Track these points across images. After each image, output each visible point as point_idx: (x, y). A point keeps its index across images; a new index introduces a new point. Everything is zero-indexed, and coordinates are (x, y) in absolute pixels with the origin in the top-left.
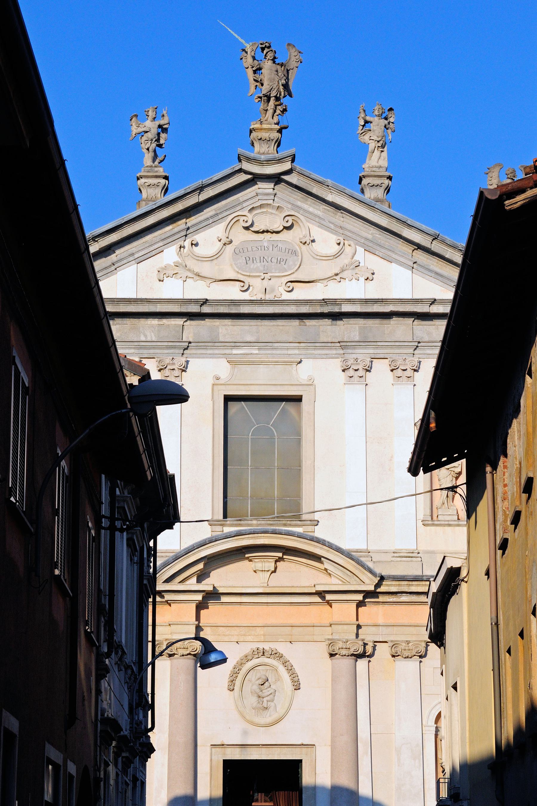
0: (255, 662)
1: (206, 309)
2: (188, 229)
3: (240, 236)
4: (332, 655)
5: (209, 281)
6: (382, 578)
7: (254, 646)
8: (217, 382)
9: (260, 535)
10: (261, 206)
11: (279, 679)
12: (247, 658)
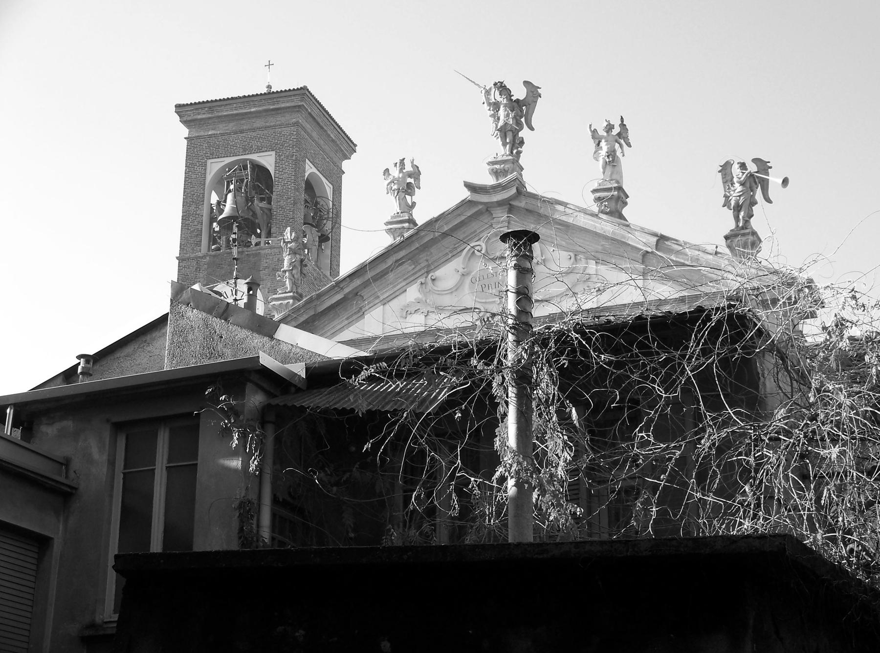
2: (429, 266)
3: (479, 265)
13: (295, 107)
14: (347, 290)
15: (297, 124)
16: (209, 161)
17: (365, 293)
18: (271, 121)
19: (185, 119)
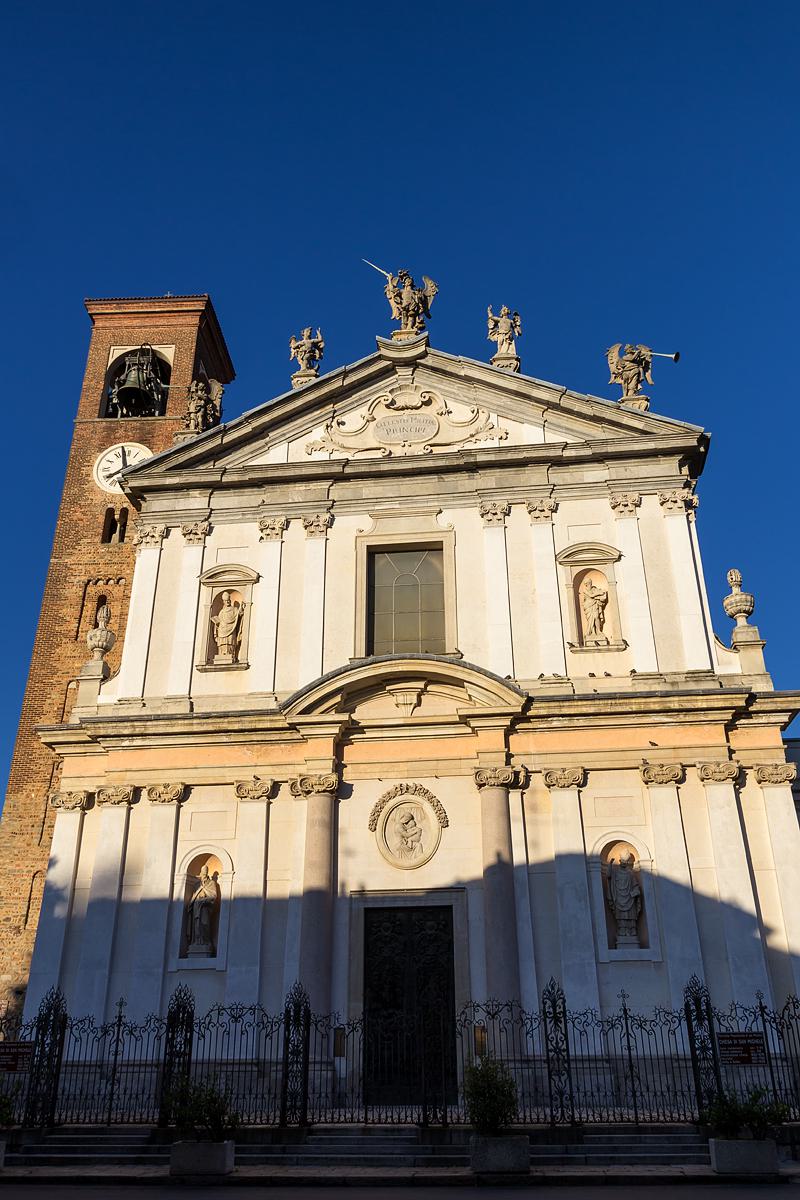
0: (399, 799)
1: (348, 470)
2: (335, 411)
3: (381, 412)
4: (481, 786)
5: (353, 452)
6: (530, 700)
7: (397, 783)
8: (361, 534)
9: (398, 661)
10: (400, 388)
11: (424, 817)
12: (390, 796)
16: (112, 348)
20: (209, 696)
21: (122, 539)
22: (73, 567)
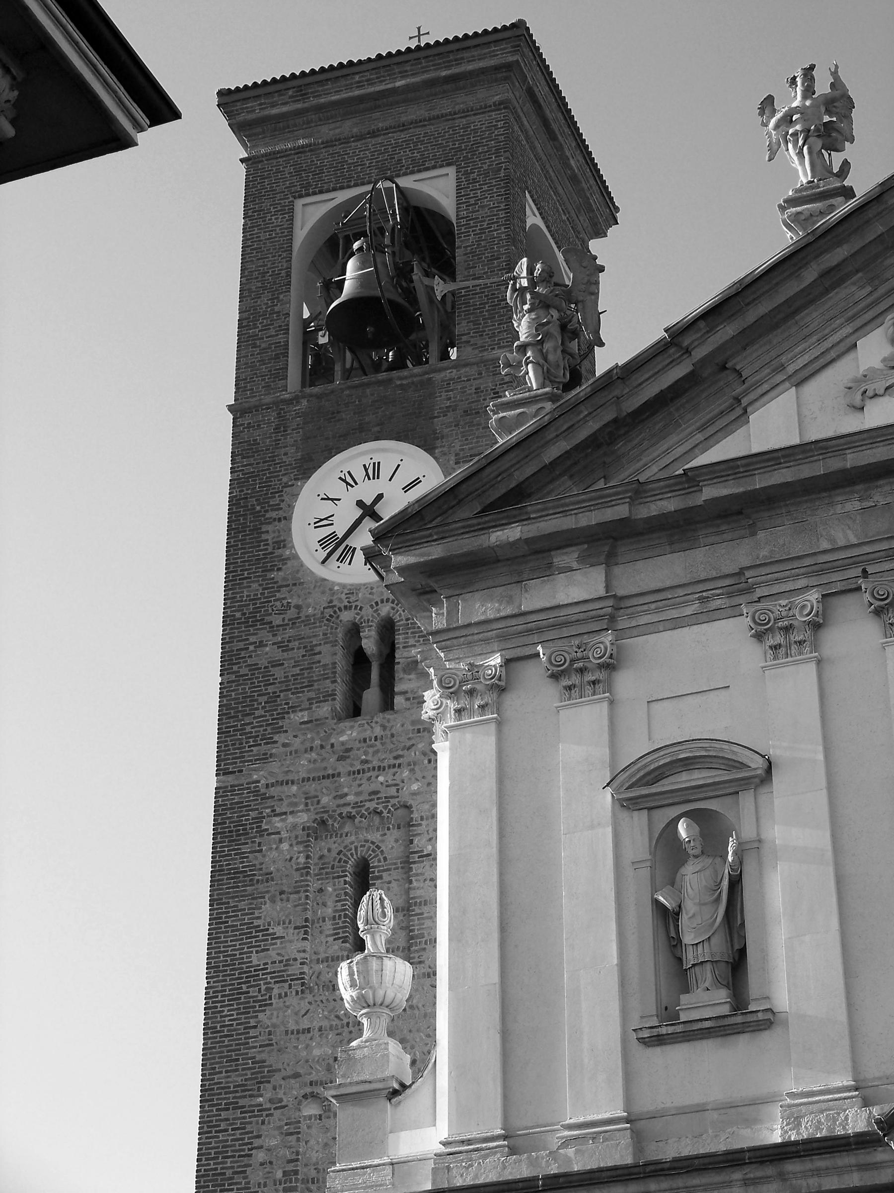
13: (497, 68)
14: (699, 353)
15: (504, 104)
17: (746, 363)
18: (444, 106)
19: (241, 118)
20: (683, 1111)
21: (387, 704)
22: (273, 791)
